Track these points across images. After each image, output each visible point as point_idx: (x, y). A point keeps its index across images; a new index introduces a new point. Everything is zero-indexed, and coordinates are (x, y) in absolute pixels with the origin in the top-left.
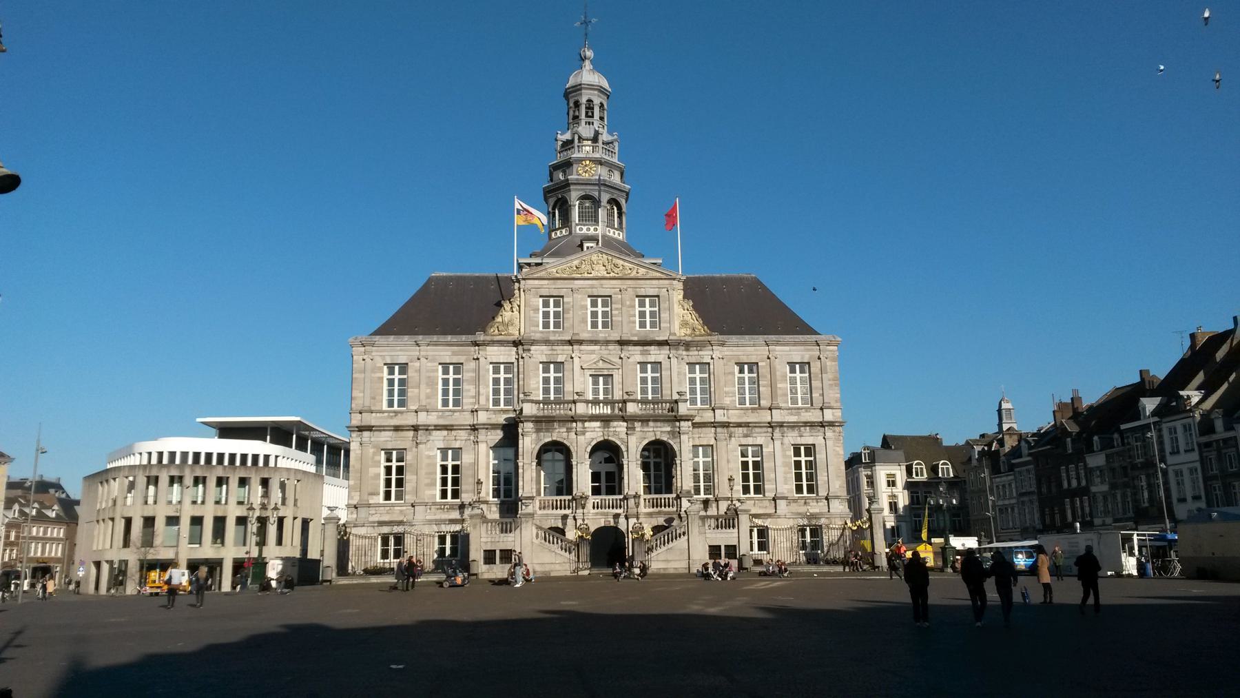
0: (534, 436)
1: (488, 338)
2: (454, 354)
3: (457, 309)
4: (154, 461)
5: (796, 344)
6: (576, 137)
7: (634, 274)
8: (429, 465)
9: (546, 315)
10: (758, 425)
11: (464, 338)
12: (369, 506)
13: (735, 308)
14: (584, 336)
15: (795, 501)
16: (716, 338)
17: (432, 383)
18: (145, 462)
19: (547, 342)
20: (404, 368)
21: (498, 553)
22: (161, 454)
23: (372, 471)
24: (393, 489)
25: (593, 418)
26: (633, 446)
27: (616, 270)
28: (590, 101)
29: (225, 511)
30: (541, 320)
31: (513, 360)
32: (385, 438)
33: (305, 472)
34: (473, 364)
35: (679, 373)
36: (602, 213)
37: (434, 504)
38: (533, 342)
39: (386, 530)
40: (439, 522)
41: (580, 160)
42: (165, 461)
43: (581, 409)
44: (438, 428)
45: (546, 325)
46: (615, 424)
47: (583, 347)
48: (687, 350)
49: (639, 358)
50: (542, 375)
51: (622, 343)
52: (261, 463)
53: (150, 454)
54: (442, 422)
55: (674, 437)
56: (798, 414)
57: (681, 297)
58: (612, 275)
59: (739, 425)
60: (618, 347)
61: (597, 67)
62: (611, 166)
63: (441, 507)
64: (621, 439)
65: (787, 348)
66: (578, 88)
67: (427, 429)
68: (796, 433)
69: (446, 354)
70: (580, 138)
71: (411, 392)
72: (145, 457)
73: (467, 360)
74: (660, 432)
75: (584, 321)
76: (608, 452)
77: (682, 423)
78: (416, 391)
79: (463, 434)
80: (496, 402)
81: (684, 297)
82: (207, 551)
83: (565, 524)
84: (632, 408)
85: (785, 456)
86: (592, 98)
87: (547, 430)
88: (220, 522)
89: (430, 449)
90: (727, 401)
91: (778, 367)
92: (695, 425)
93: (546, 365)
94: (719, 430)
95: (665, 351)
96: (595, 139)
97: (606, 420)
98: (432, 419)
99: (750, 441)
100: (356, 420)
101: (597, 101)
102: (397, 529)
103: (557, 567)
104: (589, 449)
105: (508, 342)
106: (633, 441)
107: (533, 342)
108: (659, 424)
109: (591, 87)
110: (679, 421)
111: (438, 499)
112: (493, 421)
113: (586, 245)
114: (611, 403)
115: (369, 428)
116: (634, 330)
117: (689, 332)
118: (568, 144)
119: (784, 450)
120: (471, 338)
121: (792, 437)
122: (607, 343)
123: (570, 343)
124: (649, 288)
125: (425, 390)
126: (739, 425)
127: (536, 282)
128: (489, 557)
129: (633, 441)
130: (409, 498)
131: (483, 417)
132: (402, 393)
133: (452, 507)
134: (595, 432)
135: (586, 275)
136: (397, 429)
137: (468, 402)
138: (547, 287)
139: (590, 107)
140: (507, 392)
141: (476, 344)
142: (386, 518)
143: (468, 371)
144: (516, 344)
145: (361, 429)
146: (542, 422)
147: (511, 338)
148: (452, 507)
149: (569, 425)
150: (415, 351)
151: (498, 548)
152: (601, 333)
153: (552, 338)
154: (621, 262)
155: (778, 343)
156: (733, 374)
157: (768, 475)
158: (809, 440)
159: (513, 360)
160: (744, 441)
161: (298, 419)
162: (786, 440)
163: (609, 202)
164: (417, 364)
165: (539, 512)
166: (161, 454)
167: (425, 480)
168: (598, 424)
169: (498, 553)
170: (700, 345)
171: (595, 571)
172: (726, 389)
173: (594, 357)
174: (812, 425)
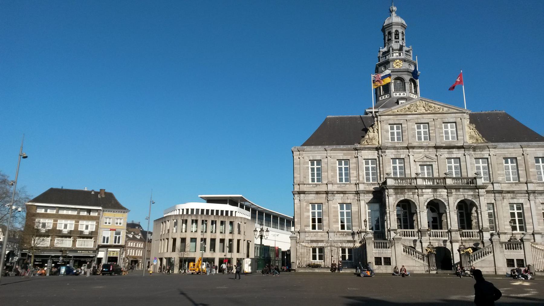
0: (394, 196)
1: (363, 146)
2: (345, 155)
3: (346, 132)
4: (185, 213)
6: (391, 49)
7: (441, 111)
8: (334, 212)
9: (392, 134)
10: (520, 192)
11: (349, 146)
12: (305, 232)
13: (496, 129)
14: (415, 144)
16: (490, 144)
17: (334, 170)
18: (181, 213)
19: (395, 148)
20: (319, 162)
21: (383, 259)
22: (187, 210)
23: (306, 214)
24: (317, 224)
25: (427, 187)
26: (452, 202)
27: (431, 109)
28: (397, 31)
29: (215, 236)
31: (376, 157)
32: (312, 197)
33: (248, 219)
34: (354, 160)
35: (471, 164)
36: (407, 86)
37: (339, 232)
38: (387, 148)
39: (314, 245)
40: (342, 242)
41: (394, 60)
42: (190, 213)
43: (420, 182)
44: (338, 192)
45: (393, 139)
46: (440, 190)
47: (414, 150)
48: (474, 151)
51: (437, 148)
52: (229, 215)
53: (183, 210)
54: (340, 190)
55: (475, 198)
57: (468, 122)
58: (428, 112)
59: (508, 192)
60: (435, 150)
61: (398, 14)
62: (410, 62)
63: (342, 234)
64: (444, 199)
65: (534, 149)
66: (390, 25)
67: (333, 193)
69: (341, 155)
70: (392, 49)
71: (324, 174)
72: (181, 211)
73: (351, 158)
74: (468, 195)
75: (414, 136)
76: (435, 207)
77: (480, 190)
78: (326, 174)
79: (351, 196)
80: (368, 179)
81: (470, 123)
82: (208, 254)
83: (415, 245)
84: (449, 182)
85: (537, 210)
86: (398, 29)
87: (402, 194)
88: (213, 241)
89: (335, 204)
90: (500, 179)
91: (529, 160)
92: (488, 192)
94: (497, 195)
95: (462, 151)
96: (401, 49)
97: (434, 188)
98: (335, 188)
99: (515, 201)
100: (297, 189)
101: (400, 31)
102: (320, 245)
103: (417, 268)
104: (426, 204)
105: (373, 148)
106: (451, 199)
107: (387, 148)
108: (466, 191)
109: (397, 24)
110: (478, 189)
111: (340, 230)
112: (367, 189)
113: (400, 102)
114: (433, 179)
115: (304, 193)
117: (474, 141)
118: (386, 53)
119: (536, 207)
120: (353, 146)
122: (428, 147)
123: (407, 148)
125: (330, 173)
126: (508, 192)
127: (387, 117)
128: (378, 261)
129: (451, 199)
130: (326, 229)
131: (362, 187)
132: (318, 175)
133: (348, 234)
134: (428, 195)
136: (317, 193)
137: (353, 180)
140: (373, 174)
141: (356, 149)
142: (314, 239)
143: (352, 164)
145: (299, 193)
146: (398, 189)
147: (374, 146)
148: (348, 234)
149: (414, 191)
150: (324, 154)
151: (382, 256)
153: (396, 146)
154: (433, 105)
155: (528, 147)
156: (502, 164)
157: (528, 220)
159: (376, 157)
160: (512, 201)
161: (241, 196)
162: (537, 201)
164: (326, 160)
166: (187, 210)
167: (332, 220)
168: (430, 190)
169: (383, 259)
170: (482, 148)
171: (440, 271)
172: (499, 172)
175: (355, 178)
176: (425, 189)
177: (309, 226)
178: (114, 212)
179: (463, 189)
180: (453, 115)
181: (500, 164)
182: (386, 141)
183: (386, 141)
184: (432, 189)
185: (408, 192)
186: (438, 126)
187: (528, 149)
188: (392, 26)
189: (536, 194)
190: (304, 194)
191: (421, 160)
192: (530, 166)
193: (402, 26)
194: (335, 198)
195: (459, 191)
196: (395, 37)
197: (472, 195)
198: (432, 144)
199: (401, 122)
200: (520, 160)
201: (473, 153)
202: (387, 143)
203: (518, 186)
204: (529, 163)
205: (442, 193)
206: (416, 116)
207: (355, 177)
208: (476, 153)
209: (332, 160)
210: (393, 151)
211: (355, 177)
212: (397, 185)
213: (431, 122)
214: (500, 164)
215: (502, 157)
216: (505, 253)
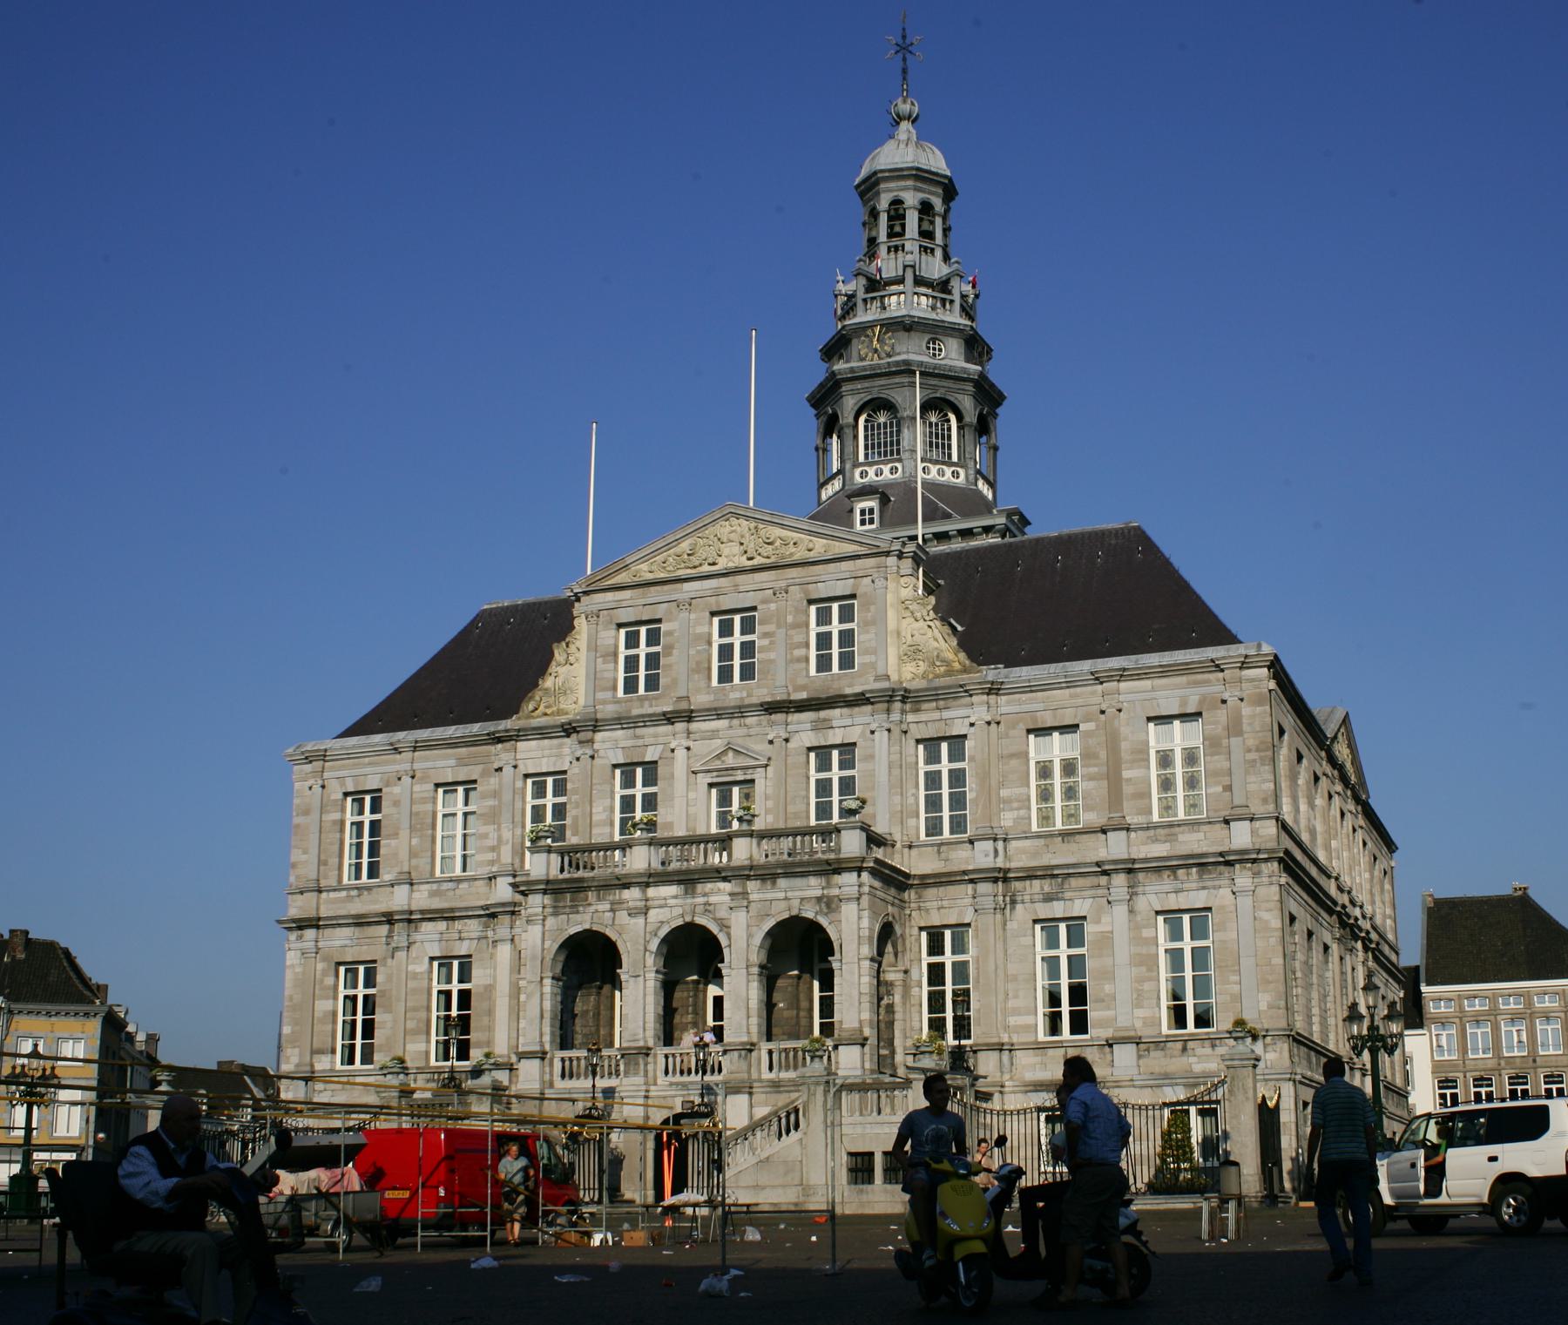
2: (461, 762)
3: (484, 676)
5: (1165, 671)
6: (862, 281)
7: (800, 554)
11: (476, 728)
13: (1050, 602)
14: (700, 700)
15: (1160, 1044)
16: (991, 673)
19: (623, 721)
28: (897, 202)
30: (621, 675)
32: (340, 941)
38: (596, 725)
47: (694, 726)
49: (810, 739)
50: (619, 792)
54: (437, 904)
56: (1171, 838)
58: (755, 562)
59: (1030, 875)
65: (1147, 684)
68: (1166, 882)
69: (445, 765)
73: (485, 774)
74: (795, 897)
78: (393, 842)
79: (473, 927)
85: (1137, 940)
90: (1007, 820)
91: (1124, 731)
93: (628, 769)
97: (688, 880)
98: (422, 898)
99: (1058, 909)
100: (298, 907)
104: (654, 945)
108: (798, 882)
109: (897, 174)
116: (810, 678)
119: (1135, 927)
120: (490, 727)
121: (1156, 893)
122: (740, 711)
123: (669, 718)
124: (832, 582)
126: (1030, 875)
127: (610, 596)
129: (739, 921)
134: (669, 907)
135: (706, 569)
136: (360, 922)
138: (631, 605)
139: (897, 212)
144: (569, 730)
145: (301, 925)
146: (563, 891)
152: (738, 690)
153: (635, 712)
154: (777, 532)
155: (1122, 675)
156: (1025, 755)
158: (1199, 899)
160: (1044, 911)
162: (1142, 903)
163: (927, 407)
164: (396, 790)
165: (560, 1084)
168: (673, 890)
172: (1004, 793)
173: (718, 745)
174: (1201, 864)
175: (490, 856)
176: (656, 884)
177: (333, 1051)
178: (48, 1014)
179: (787, 875)
180: (844, 565)
181: (1012, 756)
182: (600, 695)
183: (600, 695)
184: (679, 882)
185: (599, 899)
186: (790, 619)
187: (1123, 685)
188: (877, 183)
189: (1141, 876)
190: (318, 927)
191: (717, 764)
192: (1125, 756)
193: (917, 178)
194: (417, 937)
195: (774, 883)
196: (891, 227)
197: (819, 899)
198: (760, 692)
199: (659, 612)
200: (1088, 734)
201: (910, 718)
202: (604, 702)
203: (1073, 847)
204: (1124, 745)
205: (713, 899)
206: (713, 583)
207: (493, 849)
208: (923, 717)
209: (417, 788)
210: (621, 732)
211: (493, 849)
212: (566, 875)
213: (764, 602)
214: (1012, 756)
215: (1022, 727)
216: (845, 1130)
